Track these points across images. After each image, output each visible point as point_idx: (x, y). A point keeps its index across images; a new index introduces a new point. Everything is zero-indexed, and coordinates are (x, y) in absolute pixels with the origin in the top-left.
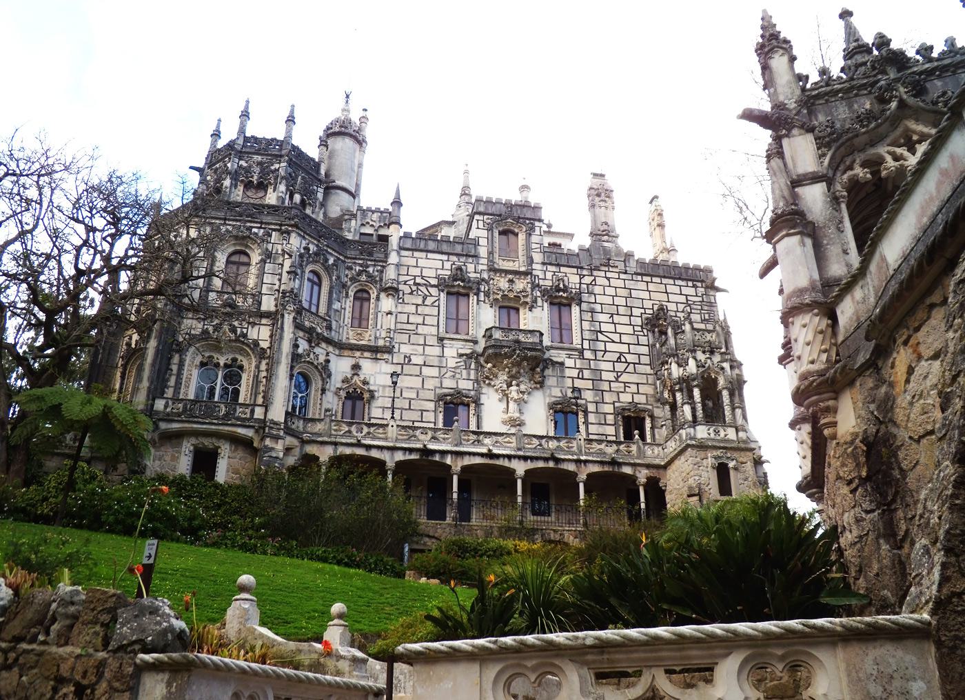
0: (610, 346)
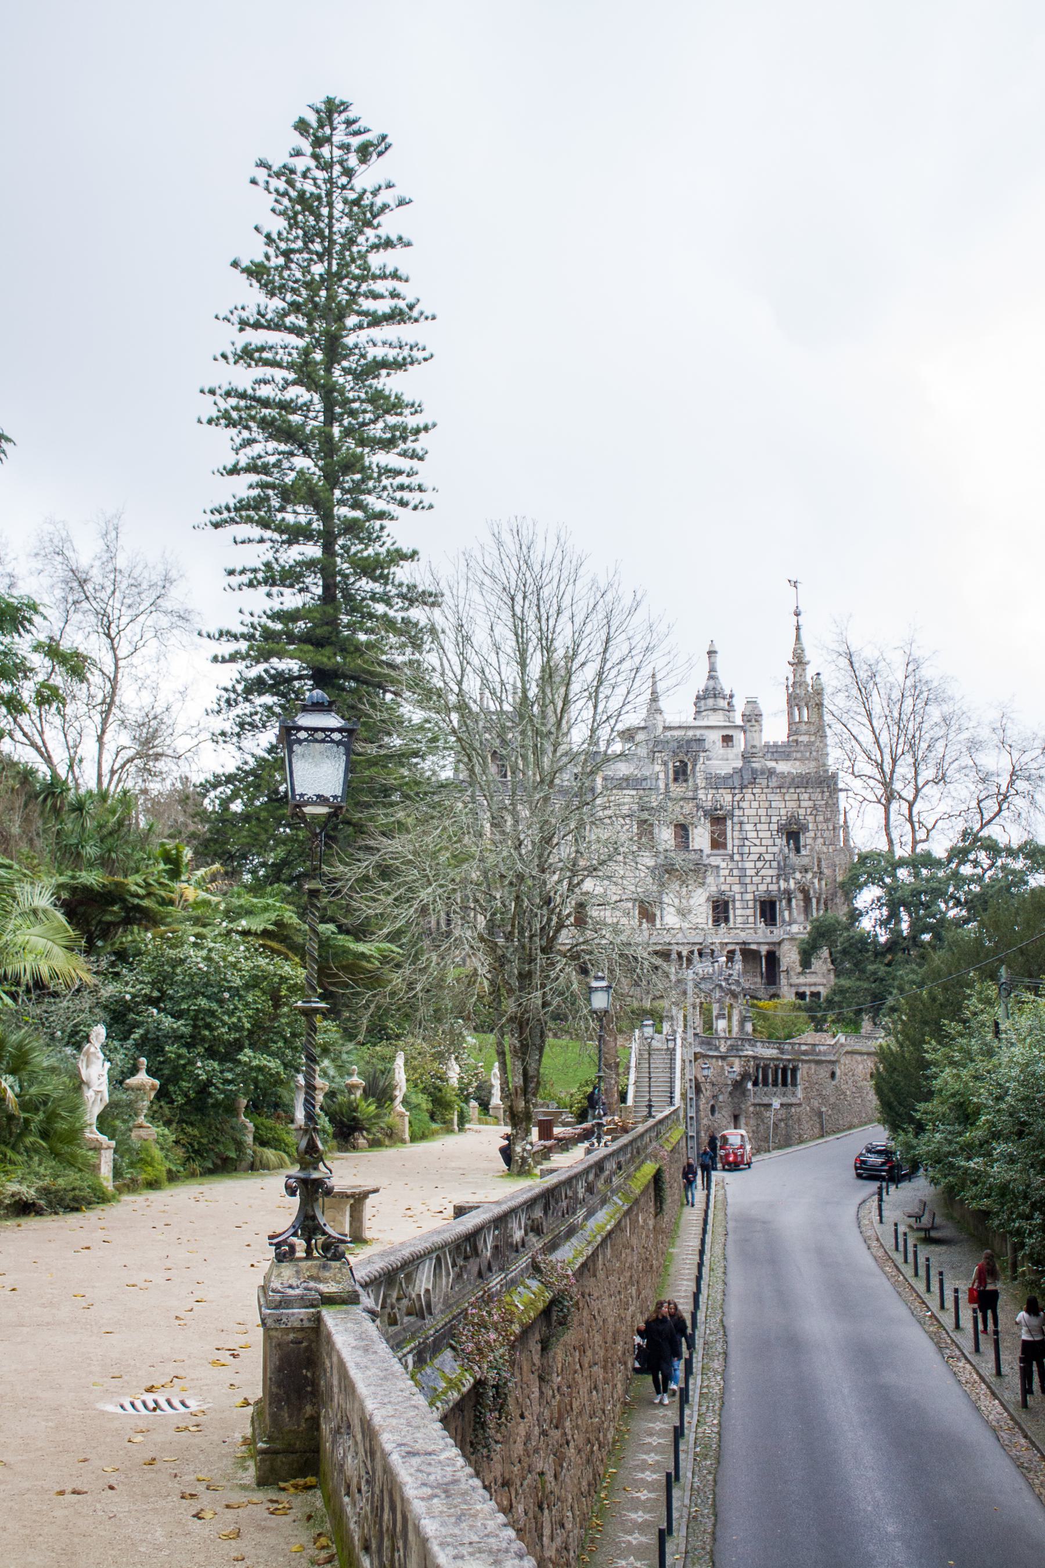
0: (753, 849)
